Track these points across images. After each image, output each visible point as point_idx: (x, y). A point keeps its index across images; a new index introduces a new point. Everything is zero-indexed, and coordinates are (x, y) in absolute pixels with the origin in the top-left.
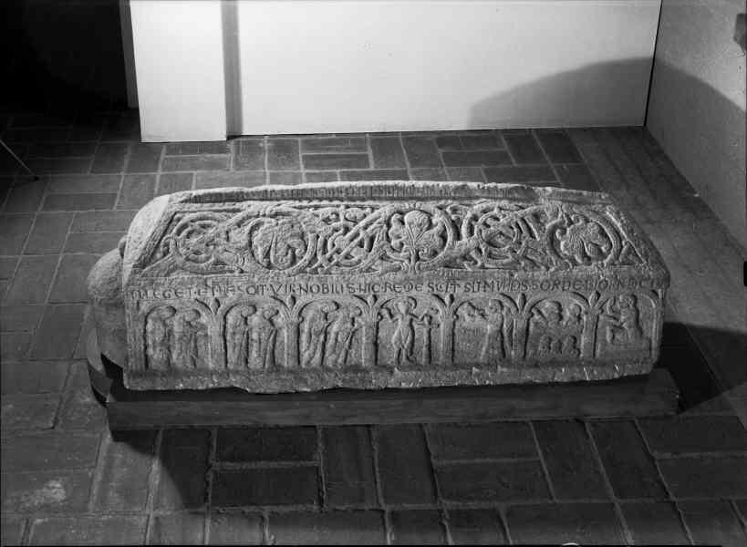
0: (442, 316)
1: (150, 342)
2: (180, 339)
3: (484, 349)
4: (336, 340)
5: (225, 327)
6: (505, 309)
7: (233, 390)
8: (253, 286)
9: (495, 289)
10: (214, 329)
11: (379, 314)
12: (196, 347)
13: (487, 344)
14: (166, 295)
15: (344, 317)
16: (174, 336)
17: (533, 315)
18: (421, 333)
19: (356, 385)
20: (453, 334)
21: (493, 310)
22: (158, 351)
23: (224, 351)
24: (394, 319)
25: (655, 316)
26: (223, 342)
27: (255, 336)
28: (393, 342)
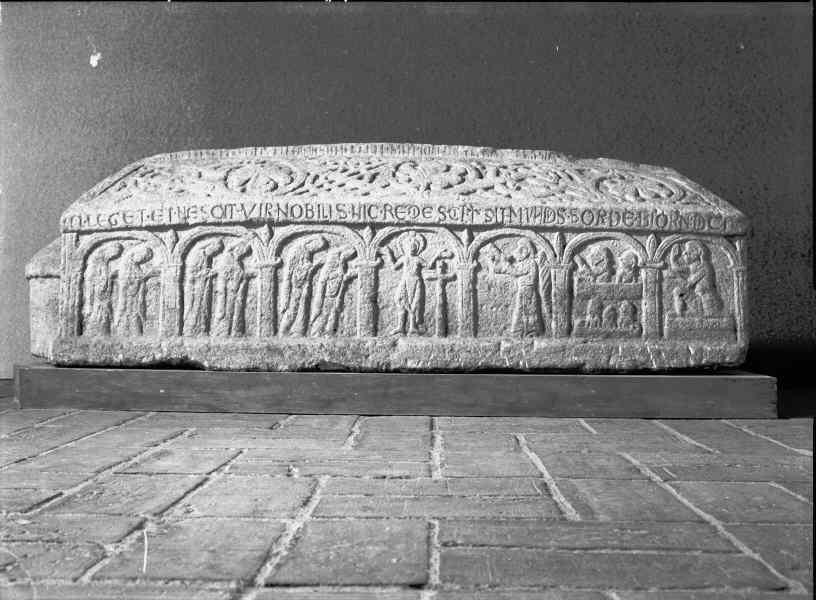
0: (460, 268)
1: (87, 295)
2: (126, 288)
3: (515, 318)
4: (323, 296)
5: (183, 268)
6: (539, 254)
7: (185, 364)
8: (221, 206)
9: (524, 219)
10: (169, 275)
11: (379, 255)
12: (144, 302)
13: (518, 306)
14: (113, 221)
15: (334, 258)
16: (117, 285)
17: (575, 267)
18: (434, 291)
19: (347, 360)
20: (475, 291)
21: (524, 255)
22: (95, 308)
23: (178, 307)
24: (398, 263)
25: (735, 278)
26: (178, 293)
27: (219, 285)
28: (397, 298)
